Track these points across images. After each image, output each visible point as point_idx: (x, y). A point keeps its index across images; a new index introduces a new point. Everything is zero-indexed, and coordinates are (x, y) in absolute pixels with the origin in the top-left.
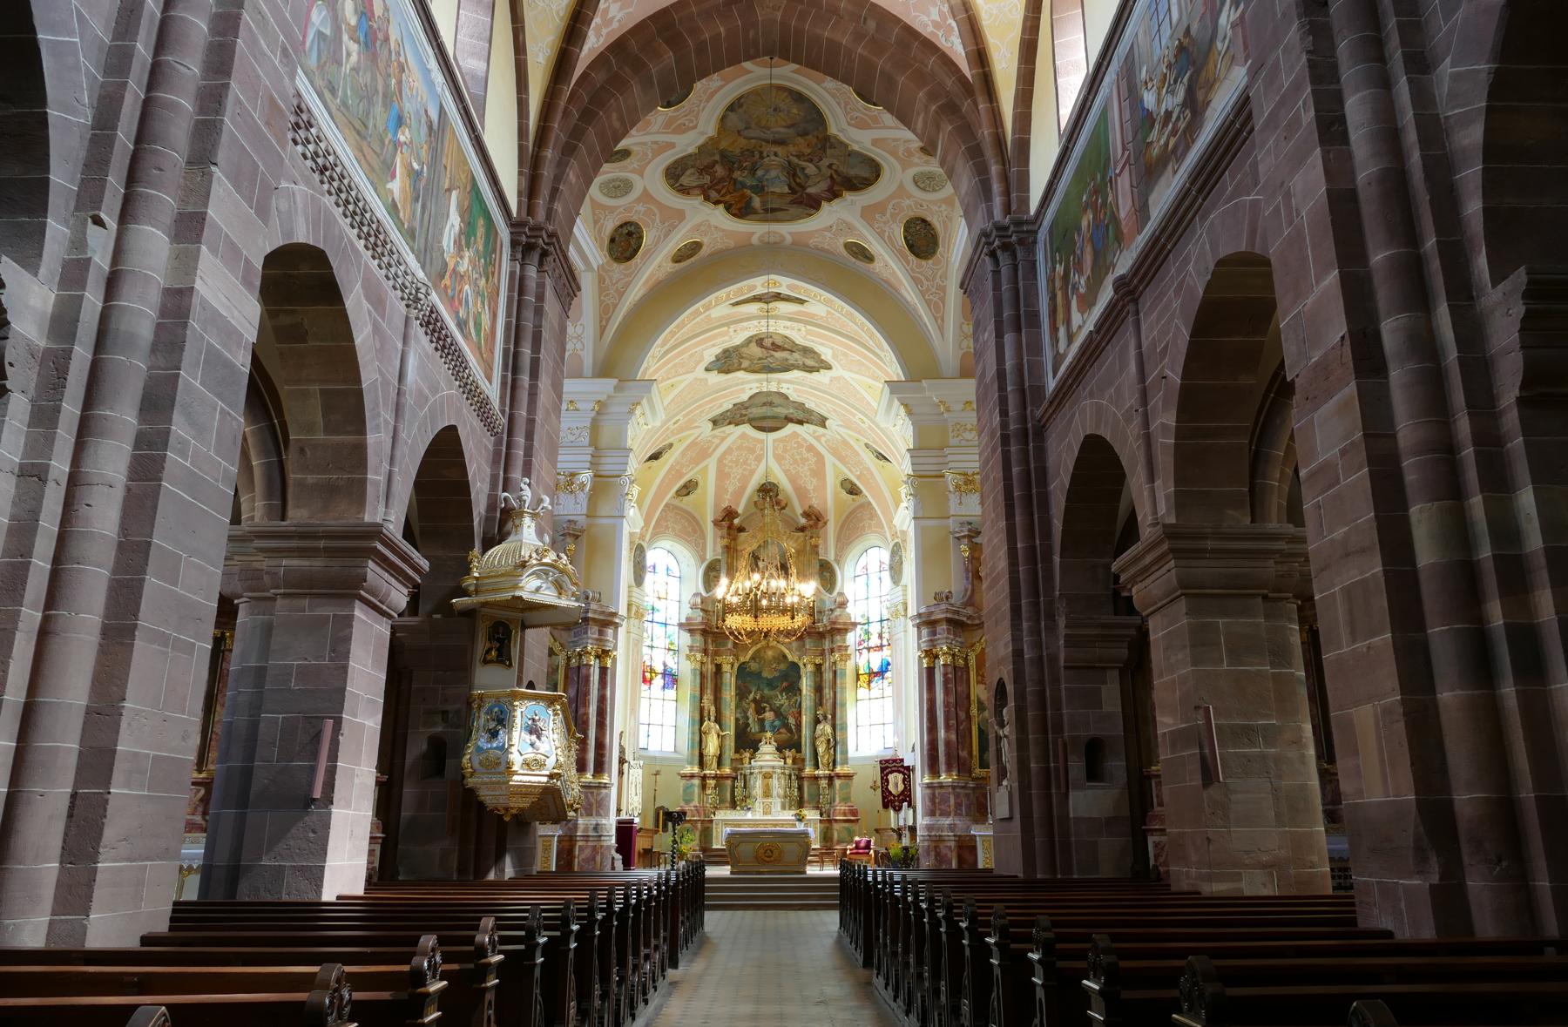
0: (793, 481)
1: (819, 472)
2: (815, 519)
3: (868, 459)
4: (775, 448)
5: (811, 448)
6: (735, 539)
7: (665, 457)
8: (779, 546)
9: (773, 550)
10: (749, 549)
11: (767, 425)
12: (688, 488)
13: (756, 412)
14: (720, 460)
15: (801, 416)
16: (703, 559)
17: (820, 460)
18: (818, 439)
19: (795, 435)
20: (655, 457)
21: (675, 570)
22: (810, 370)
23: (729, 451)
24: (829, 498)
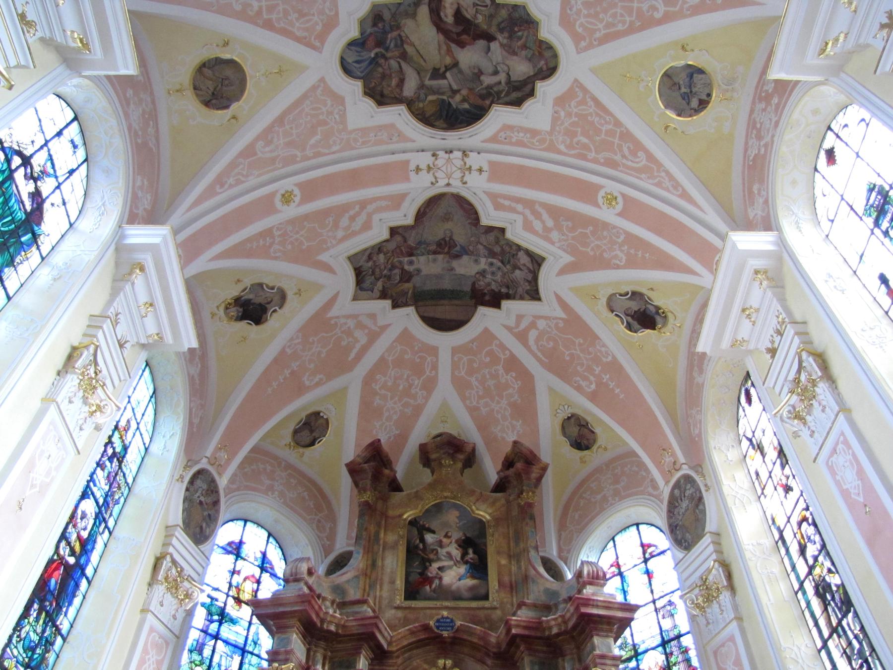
0: (482, 427)
1: (525, 409)
2: (521, 468)
3: (612, 334)
4: (455, 366)
5: (513, 363)
6: (385, 499)
7: (273, 321)
8: (464, 513)
9: (452, 517)
10: (408, 515)
11: (446, 308)
12: (311, 429)
13: (428, 267)
14: (368, 380)
15: (492, 282)
16: (327, 551)
17: (526, 378)
18: (522, 337)
19: (487, 336)
20: (252, 309)
21: (280, 567)
22: (519, 93)
23: (381, 365)
24: (549, 443)
